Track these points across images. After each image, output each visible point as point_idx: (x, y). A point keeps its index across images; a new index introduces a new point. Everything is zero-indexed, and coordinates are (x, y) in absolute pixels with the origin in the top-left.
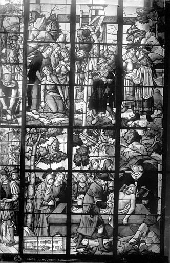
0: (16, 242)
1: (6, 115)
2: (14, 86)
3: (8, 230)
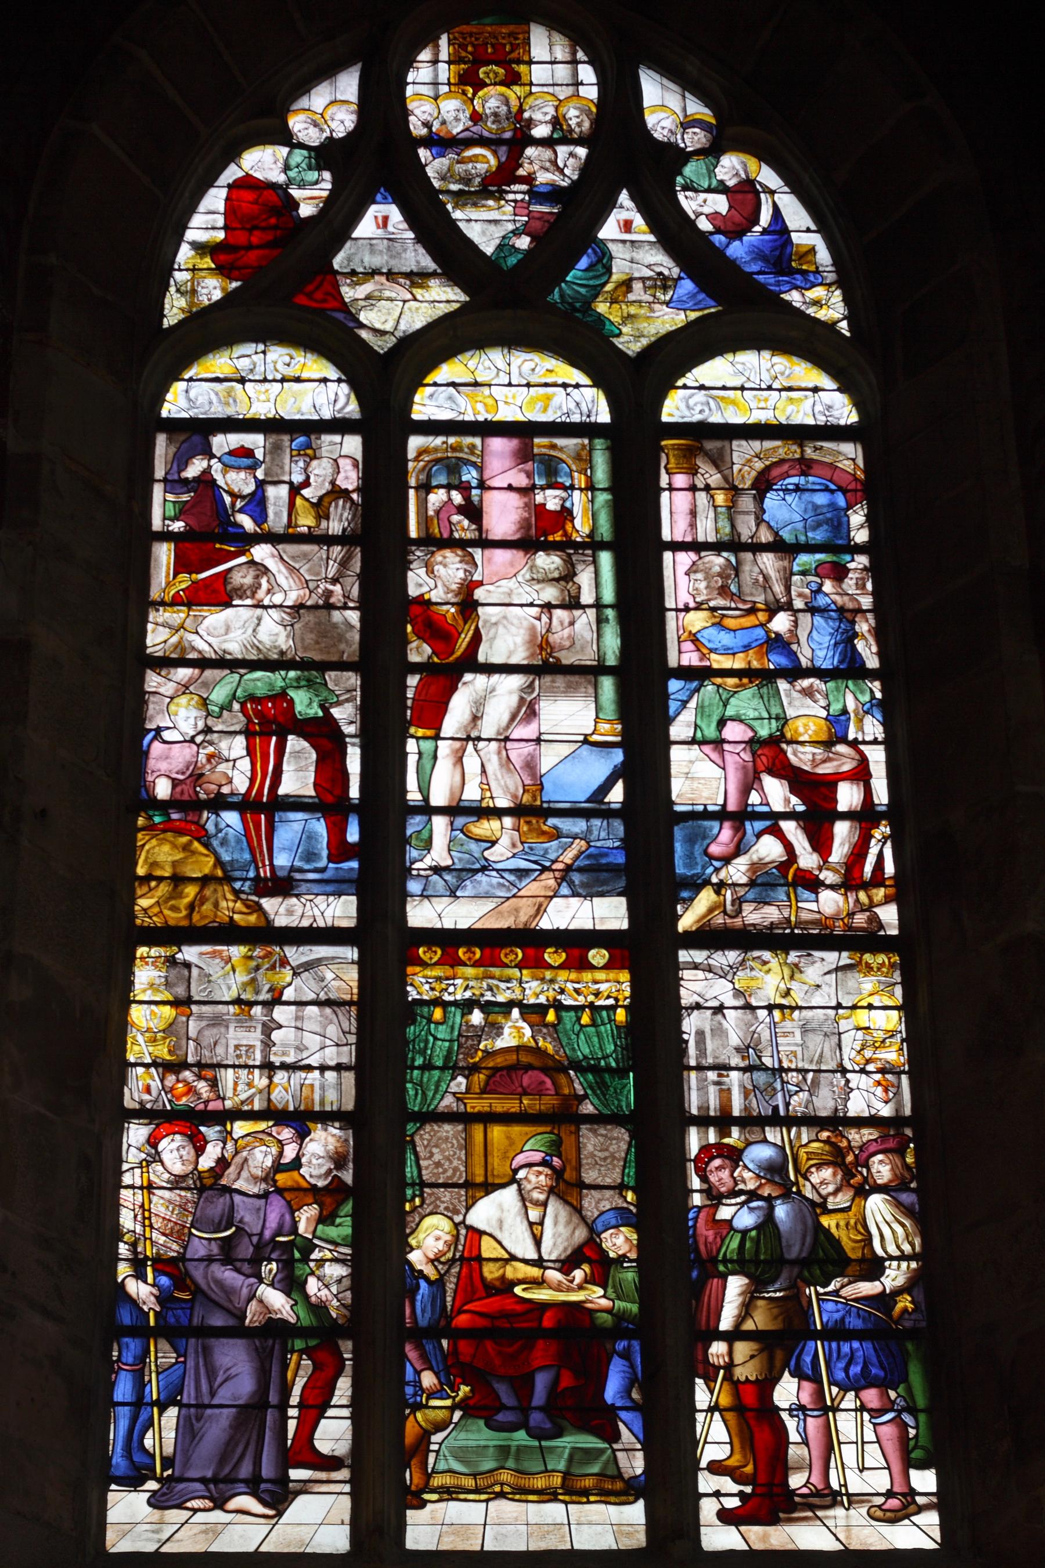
0: (920, 1500)
1: (817, 893)
2: (846, 768)
3: (869, 1435)
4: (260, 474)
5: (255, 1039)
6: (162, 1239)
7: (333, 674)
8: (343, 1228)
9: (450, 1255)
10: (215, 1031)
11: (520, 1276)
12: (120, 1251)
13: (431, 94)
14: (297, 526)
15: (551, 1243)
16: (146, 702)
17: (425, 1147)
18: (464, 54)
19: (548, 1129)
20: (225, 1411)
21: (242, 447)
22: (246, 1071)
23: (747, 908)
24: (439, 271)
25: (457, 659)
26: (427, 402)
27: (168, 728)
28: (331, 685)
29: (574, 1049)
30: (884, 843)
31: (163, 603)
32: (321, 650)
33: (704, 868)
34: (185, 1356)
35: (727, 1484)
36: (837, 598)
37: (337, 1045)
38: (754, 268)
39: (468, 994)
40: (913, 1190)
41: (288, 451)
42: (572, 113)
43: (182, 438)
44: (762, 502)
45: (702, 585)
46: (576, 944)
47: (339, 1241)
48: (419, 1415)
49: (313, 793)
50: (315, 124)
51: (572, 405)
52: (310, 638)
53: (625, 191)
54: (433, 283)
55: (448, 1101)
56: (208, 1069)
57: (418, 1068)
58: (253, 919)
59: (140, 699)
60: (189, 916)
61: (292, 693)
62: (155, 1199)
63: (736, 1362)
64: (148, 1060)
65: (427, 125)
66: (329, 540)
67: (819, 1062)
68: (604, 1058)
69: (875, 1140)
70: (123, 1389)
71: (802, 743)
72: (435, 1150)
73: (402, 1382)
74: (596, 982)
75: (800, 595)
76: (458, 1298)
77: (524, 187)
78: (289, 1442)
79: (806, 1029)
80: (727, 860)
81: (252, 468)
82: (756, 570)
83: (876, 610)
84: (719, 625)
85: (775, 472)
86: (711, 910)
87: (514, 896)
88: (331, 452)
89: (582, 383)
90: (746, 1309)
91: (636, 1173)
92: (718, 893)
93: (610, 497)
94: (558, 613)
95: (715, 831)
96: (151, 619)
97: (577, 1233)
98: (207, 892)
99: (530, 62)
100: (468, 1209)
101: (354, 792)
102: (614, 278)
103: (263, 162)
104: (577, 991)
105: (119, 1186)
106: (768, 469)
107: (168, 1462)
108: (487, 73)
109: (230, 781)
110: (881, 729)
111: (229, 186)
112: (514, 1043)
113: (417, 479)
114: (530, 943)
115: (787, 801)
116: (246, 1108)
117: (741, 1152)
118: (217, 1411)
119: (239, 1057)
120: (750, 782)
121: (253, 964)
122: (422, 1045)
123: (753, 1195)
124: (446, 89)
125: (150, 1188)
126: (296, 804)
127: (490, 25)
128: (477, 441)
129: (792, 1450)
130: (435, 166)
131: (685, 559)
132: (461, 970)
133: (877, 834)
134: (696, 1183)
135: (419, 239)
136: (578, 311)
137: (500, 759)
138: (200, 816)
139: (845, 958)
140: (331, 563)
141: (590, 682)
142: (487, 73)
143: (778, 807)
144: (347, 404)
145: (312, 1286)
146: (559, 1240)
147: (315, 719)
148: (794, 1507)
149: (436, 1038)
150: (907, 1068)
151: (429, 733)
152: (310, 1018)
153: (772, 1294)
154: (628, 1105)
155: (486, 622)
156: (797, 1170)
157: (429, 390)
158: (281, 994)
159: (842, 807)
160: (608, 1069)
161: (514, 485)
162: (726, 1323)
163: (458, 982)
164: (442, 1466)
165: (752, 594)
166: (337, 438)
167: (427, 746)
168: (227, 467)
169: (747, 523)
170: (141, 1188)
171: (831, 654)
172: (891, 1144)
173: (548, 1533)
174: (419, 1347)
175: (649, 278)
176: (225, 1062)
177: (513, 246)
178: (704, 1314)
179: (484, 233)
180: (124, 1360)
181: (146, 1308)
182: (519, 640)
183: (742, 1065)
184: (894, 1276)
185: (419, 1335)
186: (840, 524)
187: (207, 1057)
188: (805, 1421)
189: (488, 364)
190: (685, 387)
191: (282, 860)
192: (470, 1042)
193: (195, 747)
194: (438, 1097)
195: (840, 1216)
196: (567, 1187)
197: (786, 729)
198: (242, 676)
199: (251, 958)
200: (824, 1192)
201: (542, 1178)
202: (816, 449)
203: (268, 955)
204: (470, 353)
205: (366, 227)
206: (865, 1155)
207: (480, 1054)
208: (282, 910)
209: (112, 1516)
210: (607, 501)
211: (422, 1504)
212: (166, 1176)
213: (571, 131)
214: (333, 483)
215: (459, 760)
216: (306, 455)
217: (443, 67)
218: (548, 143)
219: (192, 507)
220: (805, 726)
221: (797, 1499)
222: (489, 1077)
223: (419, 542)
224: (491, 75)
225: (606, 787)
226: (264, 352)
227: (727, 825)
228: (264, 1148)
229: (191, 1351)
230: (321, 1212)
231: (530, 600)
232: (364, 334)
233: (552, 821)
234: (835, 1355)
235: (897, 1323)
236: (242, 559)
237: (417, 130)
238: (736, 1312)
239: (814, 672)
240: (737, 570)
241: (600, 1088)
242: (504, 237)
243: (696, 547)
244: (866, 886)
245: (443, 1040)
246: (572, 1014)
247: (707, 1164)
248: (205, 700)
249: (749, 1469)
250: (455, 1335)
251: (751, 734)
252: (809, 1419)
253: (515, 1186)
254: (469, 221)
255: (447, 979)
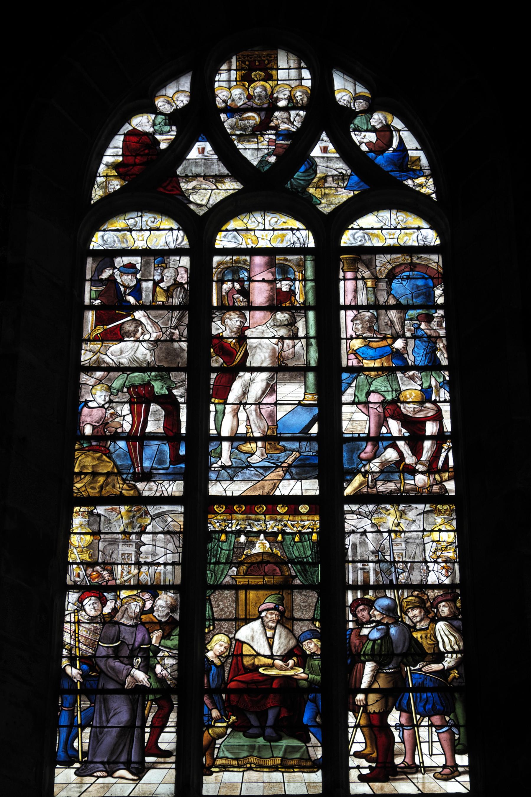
1: (414, 476)
2: (430, 414)
3: (435, 738)
4: (138, 276)
5: (132, 550)
6: (84, 647)
7: (174, 373)
8: (174, 641)
9: (227, 653)
10: (112, 547)
11: (262, 663)
12: (64, 653)
13: (227, 87)
14: (157, 301)
15: (277, 647)
16: (80, 389)
17: (216, 602)
18: (244, 66)
19: (277, 592)
20: (114, 729)
21: (130, 263)
22: (127, 566)
23: (379, 484)
24: (230, 174)
25: (236, 364)
26: (223, 239)
27: (91, 401)
28: (172, 379)
29: (291, 554)
30: (449, 451)
31: (89, 340)
32: (168, 362)
33: (358, 465)
34: (95, 703)
35: (364, 763)
36: (428, 331)
37: (173, 553)
38: (389, 169)
39: (238, 527)
40: (460, 619)
41: (153, 264)
42: (298, 94)
43: (100, 260)
44: (391, 285)
45: (360, 327)
46: (293, 502)
47: (172, 647)
48: (210, 731)
49: (163, 431)
50: (169, 103)
51: (295, 239)
52: (162, 355)
53: (324, 132)
54: (227, 180)
55: (228, 579)
56: (108, 565)
57: (213, 563)
58: (132, 492)
59: (77, 387)
60: (100, 492)
61: (153, 383)
62: (81, 628)
63: (369, 703)
64: (79, 561)
65: (225, 102)
66: (172, 308)
67: (414, 558)
68: (306, 557)
69: (441, 595)
70: (64, 720)
71: (409, 403)
72: (220, 603)
73: (202, 715)
74: (302, 521)
75: (409, 330)
76: (230, 674)
77: (273, 132)
78: (146, 744)
79: (407, 542)
80: (369, 461)
81: (135, 273)
82: (387, 318)
83: (447, 336)
84: (368, 346)
85: (397, 270)
86: (361, 485)
87: (262, 480)
88: (174, 265)
89: (301, 228)
90: (374, 678)
91: (321, 613)
92: (364, 476)
93: (314, 284)
94: (287, 341)
95: (364, 446)
96: (83, 348)
97: (291, 642)
98: (110, 480)
99: (278, 69)
100: (236, 631)
101: (183, 431)
102: (318, 175)
103: (142, 122)
104: (293, 526)
105: (63, 622)
106: (394, 268)
107: (85, 754)
108: (255, 75)
109: (122, 426)
110: (448, 395)
111: (125, 134)
112: (261, 551)
113: (217, 277)
114: (271, 502)
115: (400, 431)
116: (127, 584)
117: (374, 602)
118: (110, 729)
119: (124, 559)
120: (382, 422)
121: (132, 514)
122: (215, 552)
123: (379, 623)
124: (235, 83)
125: (78, 623)
126: (154, 437)
127: (257, 51)
128: (248, 258)
129: (396, 746)
130: (228, 122)
131: (351, 314)
132: (235, 516)
133: (445, 446)
134: (351, 617)
135: (220, 159)
136: (300, 193)
137: (256, 413)
138: (106, 443)
139: (428, 507)
140: (174, 319)
141: (302, 375)
142: (255, 75)
143: (395, 433)
144: (183, 241)
145: (158, 669)
146: (282, 646)
147: (164, 395)
148: (396, 773)
149: (222, 549)
150: (458, 560)
151: (221, 401)
152: (159, 540)
153: (388, 671)
154: (317, 580)
155: (250, 346)
156: (401, 611)
157: (224, 233)
158: (146, 528)
159: (428, 433)
160: (308, 563)
161: (266, 279)
162: (364, 685)
163: (234, 522)
164: (221, 755)
165: (384, 330)
166: (178, 258)
167: (220, 407)
168: (122, 273)
169: (383, 295)
170: (74, 623)
171: (423, 359)
172: (449, 597)
173: (273, 786)
174: (211, 698)
175: (335, 175)
176: (117, 562)
177: (267, 161)
178: (353, 680)
179: (253, 155)
180: (64, 705)
181: (75, 680)
182: (267, 355)
183: (375, 560)
184: (449, 661)
185: (211, 692)
186: (430, 294)
187: (108, 559)
188: (403, 732)
189: (253, 221)
190: (353, 229)
191: (147, 464)
192: (239, 551)
193: (104, 410)
194: (223, 577)
195: (423, 632)
196: (286, 620)
197: (401, 396)
198: (128, 375)
199: (130, 511)
200: (415, 621)
201: (274, 616)
202: (418, 258)
203: (139, 510)
204: (245, 215)
205: (194, 154)
206: (436, 603)
207: (244, 556)
208: (146, 488)
209: (57, 780)
210: (312, 286)
211: (211, 773)
212: (87, 617)
213: (298, 103)
214: (175, 280)
215: (236, 414)
216: (162, 266)
217: (233, 72)
218: (286, 109)
219: (105, 293)
220: (410, 394)
221: (398, 769)
222: (248, 568)
223: (217, 308)
224: (258, 76)
225: (310, 426)
226: (141, 216)
227: (369, 443)
228: (135, 603)
229: (97, 700)
230: (163, 634)
231: (273, 335)
232: (192, 206)
233: (281, 443)
234: (419, 700)
235: (450, 684)
236: (130, 318)
237: (220, 104)
238: (369, 679)
239: (415, 368)
240: (377, 318)
241: (304, 572)
242: (263, 157)
243: (357, 307)
244: (439, 472)
245: (226, 550)
246: (290, 536)
247: (357, 608)
248: (110, 387)
249: (375, 755)
250: (229, 692)
251: (382, 399)
252: (405, 731)
253: (260, 620)
254: (245, 149)
255: (228, 520)
